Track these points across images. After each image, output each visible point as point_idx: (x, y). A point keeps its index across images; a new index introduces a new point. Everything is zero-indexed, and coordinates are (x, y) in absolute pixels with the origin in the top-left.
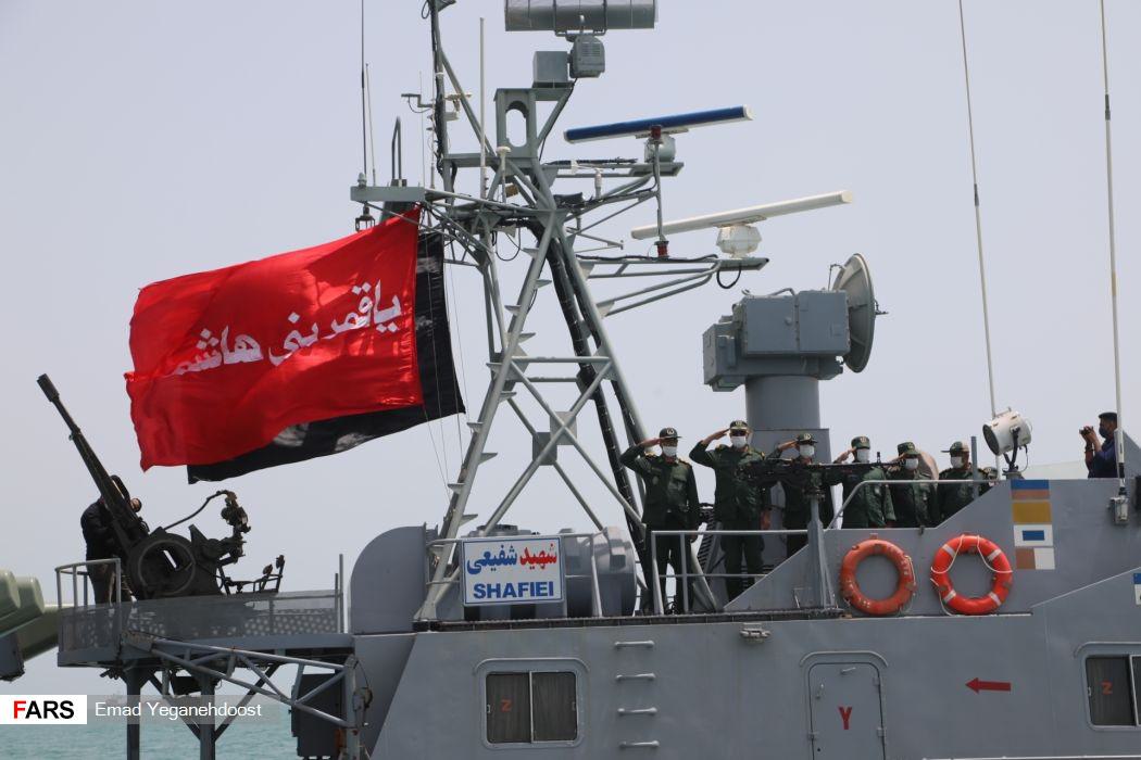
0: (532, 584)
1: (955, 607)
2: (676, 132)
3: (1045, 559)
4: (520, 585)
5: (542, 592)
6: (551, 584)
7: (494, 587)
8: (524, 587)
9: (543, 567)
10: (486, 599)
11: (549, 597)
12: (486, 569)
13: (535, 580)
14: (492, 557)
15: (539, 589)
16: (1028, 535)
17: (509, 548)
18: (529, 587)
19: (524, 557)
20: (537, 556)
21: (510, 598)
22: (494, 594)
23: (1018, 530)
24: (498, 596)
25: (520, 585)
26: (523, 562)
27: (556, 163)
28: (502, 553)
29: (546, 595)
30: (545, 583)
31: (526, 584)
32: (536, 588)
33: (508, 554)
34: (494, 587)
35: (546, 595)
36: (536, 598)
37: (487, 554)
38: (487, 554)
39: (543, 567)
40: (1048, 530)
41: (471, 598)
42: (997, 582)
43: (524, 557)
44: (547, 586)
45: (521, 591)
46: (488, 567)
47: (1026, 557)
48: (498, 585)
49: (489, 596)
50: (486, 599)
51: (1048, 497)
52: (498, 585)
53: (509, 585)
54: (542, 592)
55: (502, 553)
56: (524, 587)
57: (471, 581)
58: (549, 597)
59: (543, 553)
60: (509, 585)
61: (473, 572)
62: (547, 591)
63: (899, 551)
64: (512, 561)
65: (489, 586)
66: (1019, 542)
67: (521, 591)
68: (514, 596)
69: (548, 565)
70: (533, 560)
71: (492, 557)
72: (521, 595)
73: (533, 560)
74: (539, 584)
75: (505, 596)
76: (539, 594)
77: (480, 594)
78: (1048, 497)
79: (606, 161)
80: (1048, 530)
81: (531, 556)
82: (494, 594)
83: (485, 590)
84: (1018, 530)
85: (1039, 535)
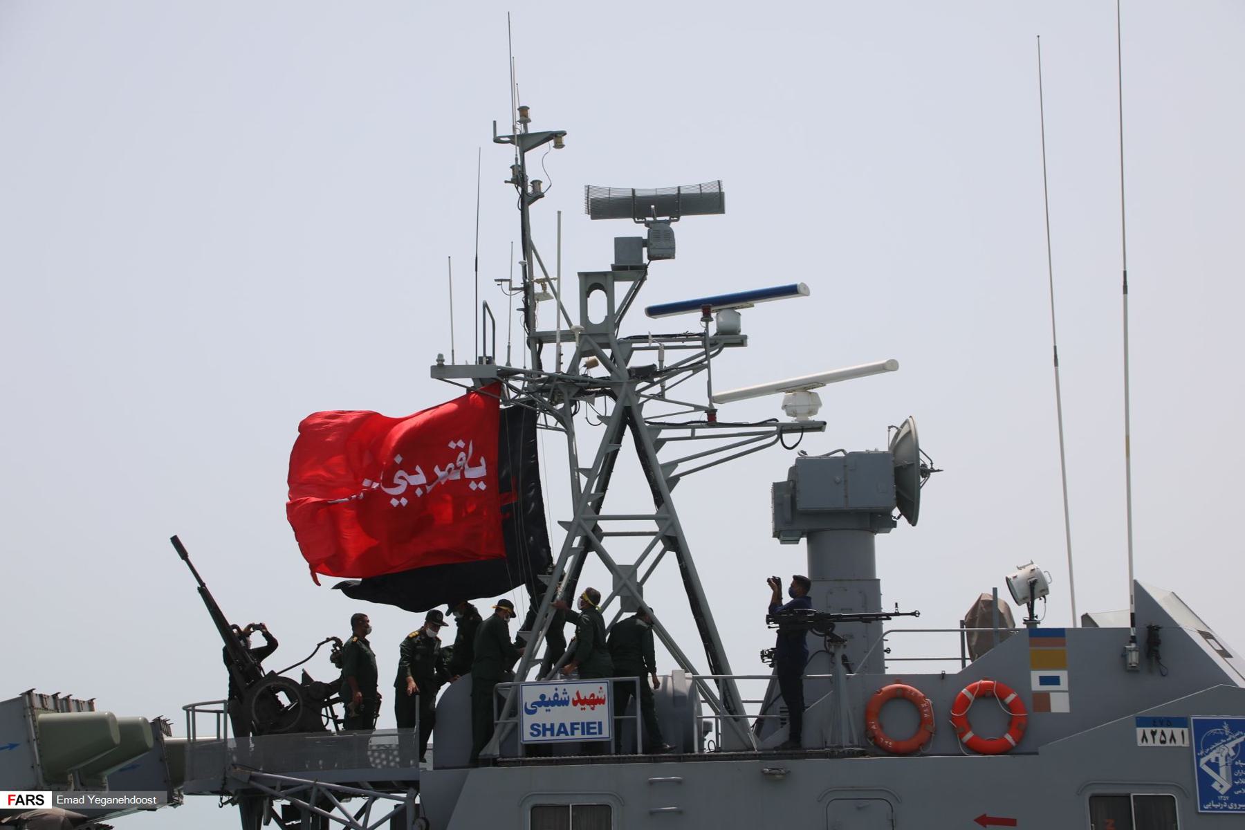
0: (583, 724)
1: (973, 748)
2: (739, 308)
3: (1060, 703)
4: (572, 724)
5: (592, 731)
6: (600, 723)
7: (548, 726)
8: (576, 726)
9: (593, 709)
10: (541, 737)
11: (598, 736)
12: (541, 710)
13: (586, 720)
14: (547, 699)
15: (589, 728)
16: (1044, 681)
17: (562, 691)
18: (580, 726)
19: (576, 699)
20: (588, 698)
21: (562, 736)
22: (548, 733)
23: (1035, 676)
24: (552, 734)
25: (572, 724)
26: (575, 703)
27: (630, 337)
28: (556, 695)
29: (595, 733)
30: (595, 723)
31: (578, 724)
32: (586, 728)
33: (562, 697)
34: (548, 726)
35: (595, 733)
36: (586, 736)
37: (543, 696)
38: (543, 696)
39: (593, 709)
40: (1063, 675)
41: (527, 736)
42: (1018, 726)
43: (576, 699)
44: (597, 726)
45: (573, 729)
46: (543, 708)
47: (1043, 701)
48: (552, 725)
49: (544, 735)
50: (541, 737)
51: (1064, 644)
52: (552, 725)
53: (562, 725)
54: (592, 731)
55: (556, 695)
56: (576, 726)
57: (527, 721)
58: (598, 736)
59: (593, 695)
60: (562, 725)
61: (530, 712)
62: (597, 730)
63: (921, 694)
64: (565, 703)
65: (544, 725)
66: (1036, 686)
67: (573, 729)
68: (567, 734)
69: (597, 706)
70: (584, 702)
71: (547, 699)
72: (573, 734)
73: (584, 702)
74: (588, 724)
75: (558, 735)
76: (589, 733)
77: (535, 733)
78: (1064, 644)
79: (675, 335)
80: (1063, 675)
81: (582, 698)
82: (548, 733)
83: (541, 729)
84: (1035, 676)
85: (1055, 681)
